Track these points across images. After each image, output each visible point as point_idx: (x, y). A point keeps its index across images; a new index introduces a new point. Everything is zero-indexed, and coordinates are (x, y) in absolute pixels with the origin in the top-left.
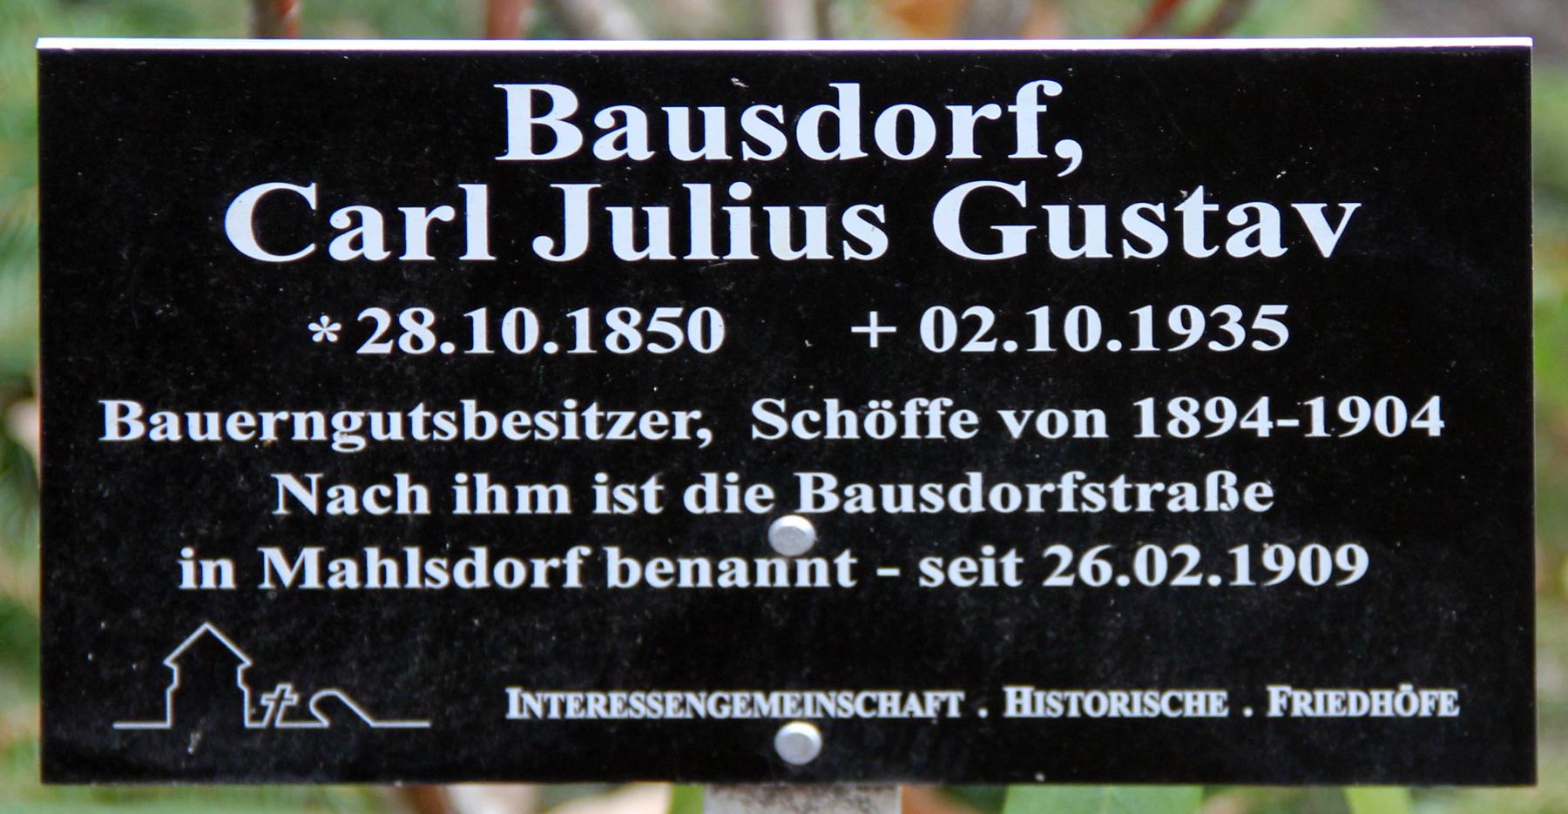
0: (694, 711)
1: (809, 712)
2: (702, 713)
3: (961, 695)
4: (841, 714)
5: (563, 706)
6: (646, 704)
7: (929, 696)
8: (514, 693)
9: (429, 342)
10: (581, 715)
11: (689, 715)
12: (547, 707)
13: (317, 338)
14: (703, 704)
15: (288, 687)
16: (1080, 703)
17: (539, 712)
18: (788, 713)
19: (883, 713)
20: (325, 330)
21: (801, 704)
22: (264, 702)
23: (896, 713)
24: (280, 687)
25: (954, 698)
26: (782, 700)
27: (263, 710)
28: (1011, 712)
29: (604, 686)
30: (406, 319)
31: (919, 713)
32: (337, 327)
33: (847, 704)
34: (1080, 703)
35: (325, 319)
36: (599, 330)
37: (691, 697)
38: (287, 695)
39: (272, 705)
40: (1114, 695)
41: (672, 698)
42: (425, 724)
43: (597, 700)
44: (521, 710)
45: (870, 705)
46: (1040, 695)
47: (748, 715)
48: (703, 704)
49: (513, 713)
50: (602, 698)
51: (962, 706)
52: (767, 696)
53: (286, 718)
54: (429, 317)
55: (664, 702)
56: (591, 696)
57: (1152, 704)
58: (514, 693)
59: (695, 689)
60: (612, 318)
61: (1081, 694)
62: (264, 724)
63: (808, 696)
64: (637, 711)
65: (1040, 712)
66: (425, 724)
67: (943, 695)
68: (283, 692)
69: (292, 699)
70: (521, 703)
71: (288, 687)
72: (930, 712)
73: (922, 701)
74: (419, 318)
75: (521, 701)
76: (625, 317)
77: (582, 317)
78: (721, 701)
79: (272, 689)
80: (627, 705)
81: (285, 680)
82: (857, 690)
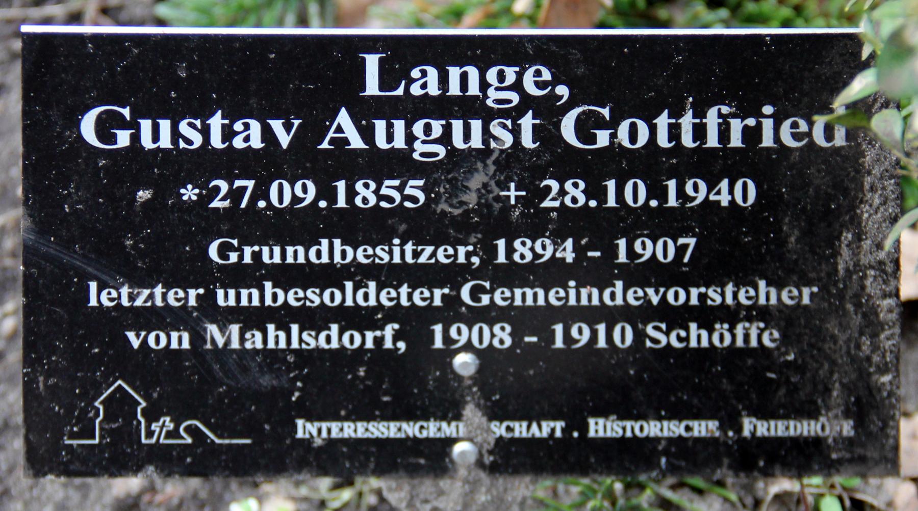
2: (411, 435)
5: (329, 431)
6: (378, 429)
7: (544, 424)
8: (300, 422)
10: (340, 436)
15: (168, 419)
18: (461, 434)
19: (517, 434)
20: (189, 193)
23: (525, 434)
25: (559, 425)
26: (457, 427)
27: (154, 431)
28: (592, 434)
31: (538, 434)
35: (190, 187)
36: (351, 193)
37: (404, 425)
38: (167, 423)
39: (158, 430)
40: (652, 423)
41: (393, 426)
42: (248, 441)
43: (349, 427)
47: (438, 435)
48: (411, 429)
49: (300, 434)
50: (352, 425)
51: (563, 430)
52: (449, 424)
53: (167, 437)
55: (388, 428)
56: (346, 424)
57: (674, 429)
58: (300, 422)
60: (359, 186)
61: (633, 423)
62: (154, 440)
64: (372, 433)
66: (248, 441)
67: (552, 424)
68: (164, 422)
69: (171, 426)
71: (168, 419)
75: (305, 427)
76: (366, 186)
77: (341, 185)
78: (422, 427)
79: (157, 420)
80: (367, 430)
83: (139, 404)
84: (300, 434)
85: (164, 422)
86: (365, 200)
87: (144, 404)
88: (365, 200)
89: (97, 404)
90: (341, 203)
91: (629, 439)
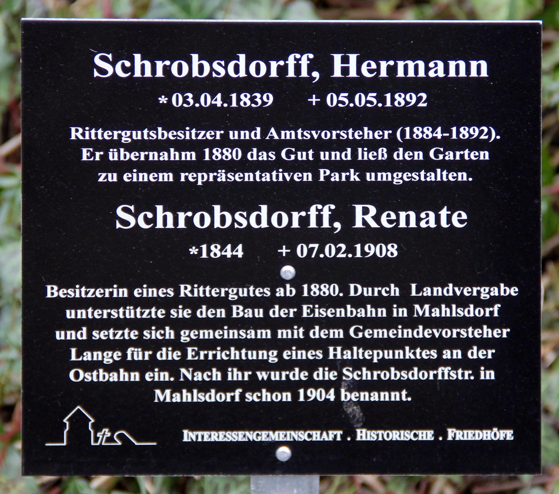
0: (248, 438)
1: (288, 439)
2: (251, 440)
3: (341, 432)
4: (300, 440)
5: (203, 437)
6: (232, 436)
8: (185, 432)
11: (247, 440)
12: (197, 437)
14: (252, 436)
15: (107, 430)
16: (383, 435)
17: (194, 440)
18: (281, 439)
19: (314, 439)
22: (98, 436)
23: (319, 439)
24: (104, 430)
25: (339, 433)
27: (99, 438)
28: (358, 439)
29: (217, 429)
31: (326, 439)
33: (301, 436)
34: (383, 435)
37: (247, 433)
38: (106, 433)
39: (101, 437)
40: (394, 432)
41: (241, 433)
43: (214, 434)
45: (310, 436)
46: (369, 432)
47: (267, 440)
48: (252, 436)
49: (185, 439)
50: (216, 434)
51: (342, 436)
52: (274, 433)
55: (238, 435)
56: (213, 433)
58: (185, 432)
59: (249, 430)
61: (383, 432)
62: (98, 444)
63: (288, 433)
64: (228, 439)
65: (369, 439)
66: (155, 444)
67: (335, 432)
68: (105, 431)
69: (109, 434)
70: (188, 436)
71: (107, 430)
72: (331, 439)
73: (328, 434)
75: (188, 434)
78: (258, 435)
79: (101, 431)
80: (225, 436)
81: (105, 427)
82: (305, 430)
83: (90, 420)
84: (185, 439)
85: (105, 431)
87: (93, 421)
89: (65, 421)
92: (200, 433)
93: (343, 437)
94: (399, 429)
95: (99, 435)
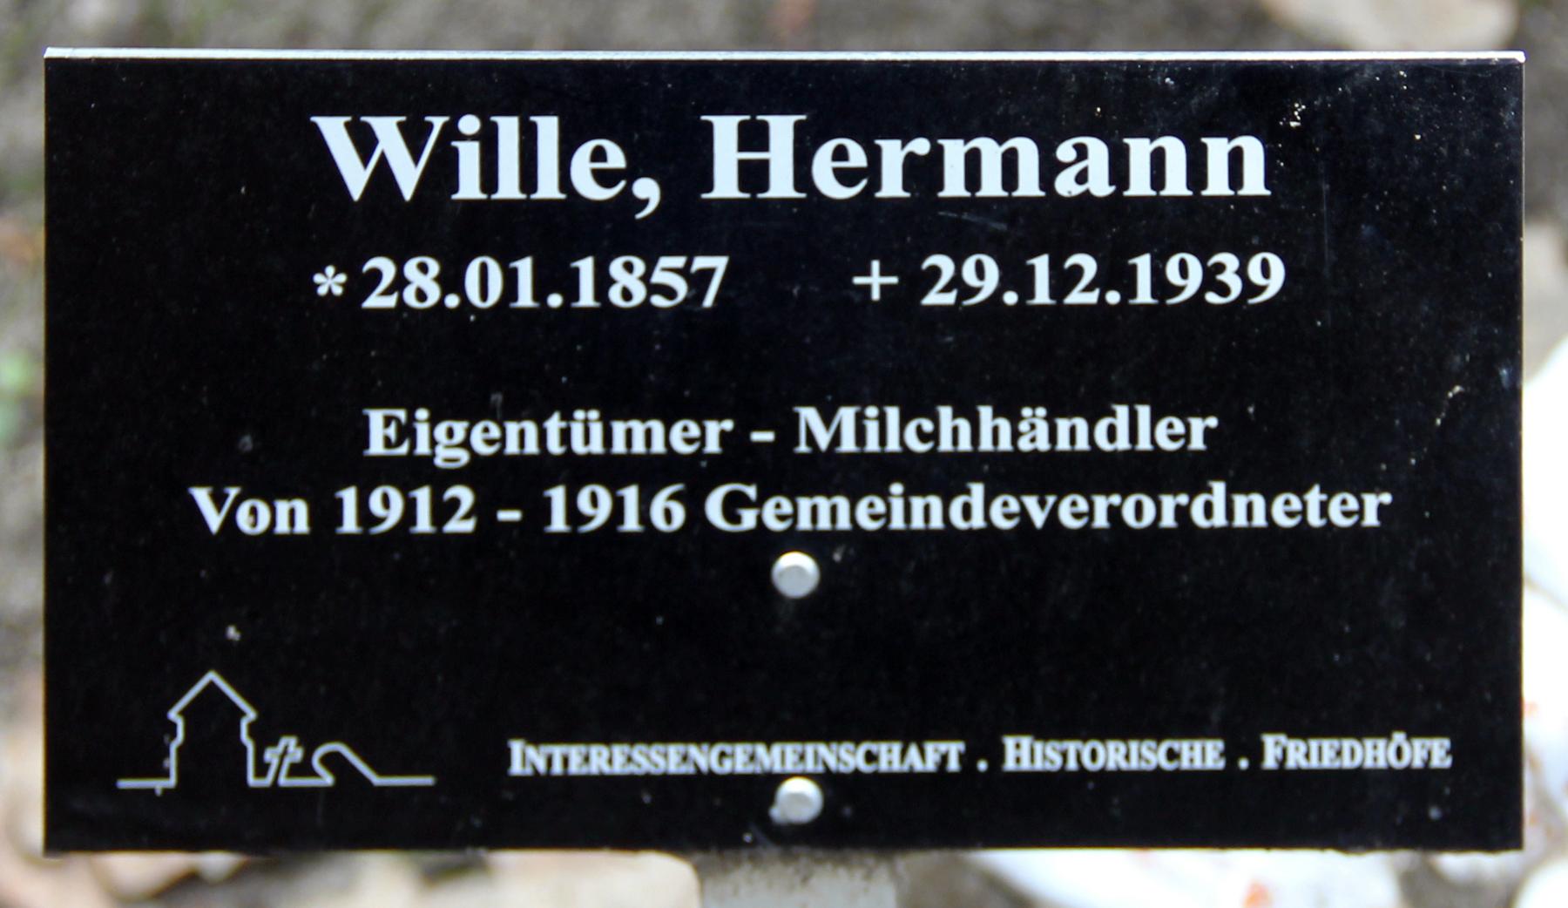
0: (696, 765)
1: (810, 766)
2: (704, 766)
4: (843, 769)
5: (566, 761)
6: (648, 757)
8: (516, 747)
9: (434, 294)
10: (584, 770)
13: (322, 291)
14: (705, 758)
18: (789, 767)
19: (883, 766)
20: (330, 282)
21: (802, 757)
23: (897, 767)
25: (954, 749)
26: (783, 754)
28: (1010, 765)
30: (411, 268)
31: (919, 766)
32: (342, 278)
33: (848, 757)
35: (330, 270)
36: (603, 282)
37: (693, 750)
40: (1112, 745)
41: (674, 750)
44: (524, 764)
46: (1039, 746)
47: (751, 769)
48: (705, 758)
49: (517, 768)
50: (604, 750)
51: (962, 758)
54: (434, 267)
55: (666, 756)
57: (1147, 755)
58: (516, 747)
60: (616, 268)
62: (267, 781)
63: (810, 748)
66: (427, 781)
67: (943, 746)
68: (286, 748)
69: (296, 754)
70: (525, 758)
74: (423, 268)
75: (524, 755)
76: (629, 267)
77: (586, 266)
78: (723, 755)
79: (275, 743)
80: (630, 759)
81: (289, 733)
83: (242, 714)
85: (286, 748)
86: (627, 294)
87: (251, 715)
88: (627, 294)
89: (174, 714)
90: (587, 298)
91: (1072, 773)
92: (557, 751)
93: (967, 759)
94: (1125, 736)
95: (271, 755)
